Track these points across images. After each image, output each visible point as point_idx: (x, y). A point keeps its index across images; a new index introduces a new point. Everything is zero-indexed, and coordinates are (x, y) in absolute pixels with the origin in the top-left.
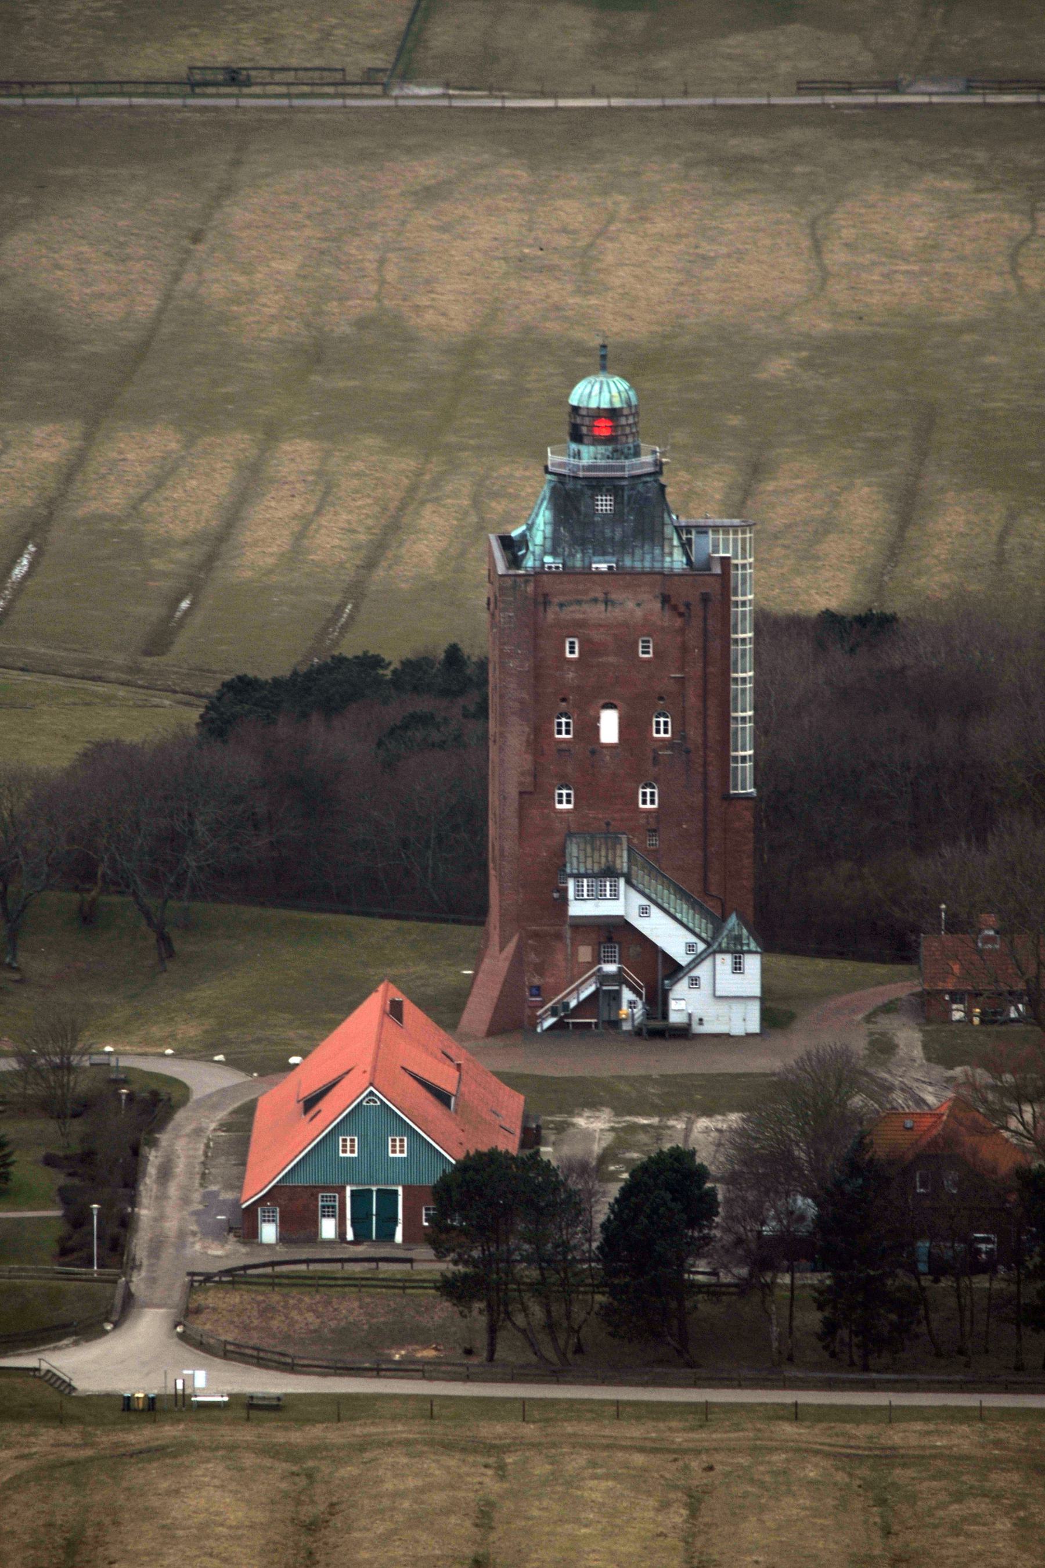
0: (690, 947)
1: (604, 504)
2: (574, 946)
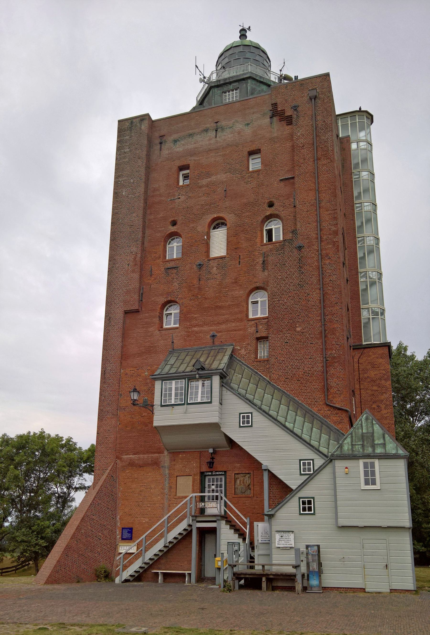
0: (304, 463)
1: (232, 96)
2: (173, 478)
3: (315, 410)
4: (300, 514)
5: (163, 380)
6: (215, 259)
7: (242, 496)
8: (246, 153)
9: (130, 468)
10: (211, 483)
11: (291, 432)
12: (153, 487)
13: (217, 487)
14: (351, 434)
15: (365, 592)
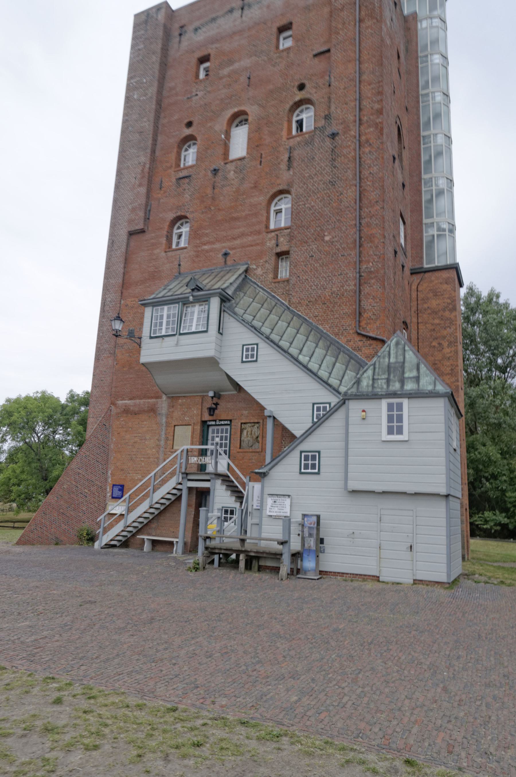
3: (342, 341)
4: (301, 473)
5: (153, 306)
6: (232, 161)
7: (248, 450)
8: (275, 30)
9: (125, 415)
10: (215, 435)
11: (305, 368)
12: (148, 438)
13: (221, 439)
14: (374, 364)
15: (379, 581)
